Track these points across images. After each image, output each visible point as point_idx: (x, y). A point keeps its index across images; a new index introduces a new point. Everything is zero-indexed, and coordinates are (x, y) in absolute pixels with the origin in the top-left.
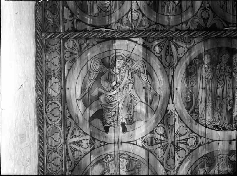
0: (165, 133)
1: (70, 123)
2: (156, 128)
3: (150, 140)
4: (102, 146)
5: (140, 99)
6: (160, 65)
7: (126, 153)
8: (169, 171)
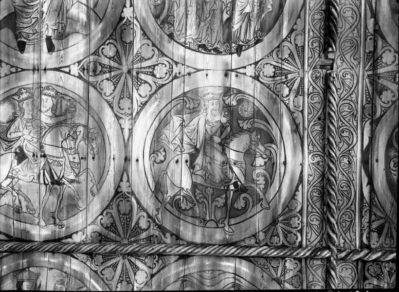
0: (117, 55)
3: (91, 65)
4: (12, 73)
7: (52, 86)
8: (123, 118)
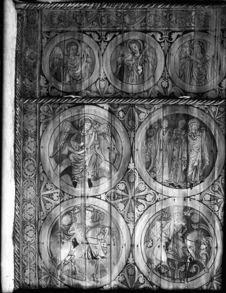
1: (43, 178)
4: (70, 199)
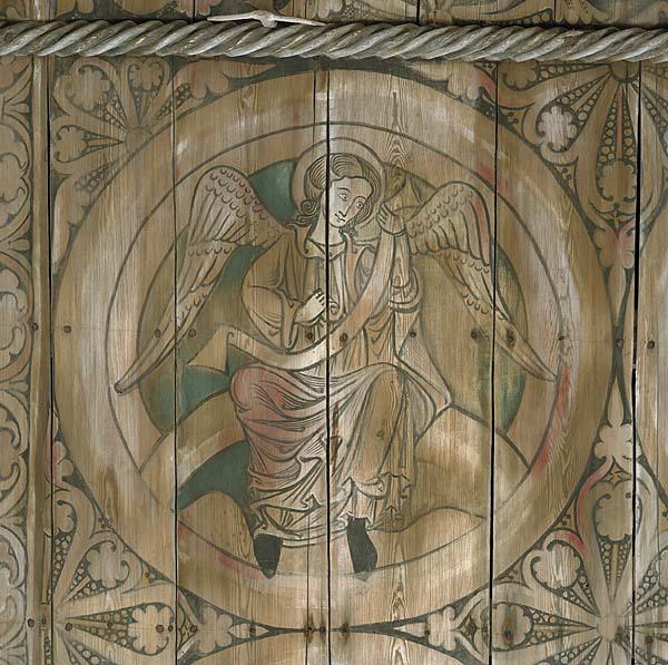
1: (74, 517)
2: (537, 553)
3: (499, 615)
4: (237, 641)
5: (453, 395)
6: (565, 216)
